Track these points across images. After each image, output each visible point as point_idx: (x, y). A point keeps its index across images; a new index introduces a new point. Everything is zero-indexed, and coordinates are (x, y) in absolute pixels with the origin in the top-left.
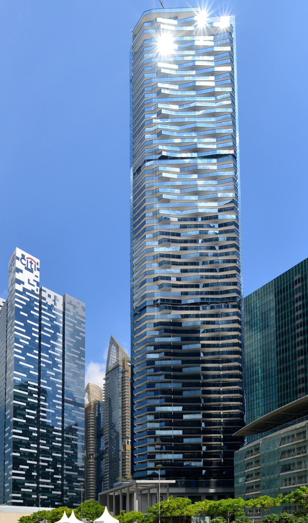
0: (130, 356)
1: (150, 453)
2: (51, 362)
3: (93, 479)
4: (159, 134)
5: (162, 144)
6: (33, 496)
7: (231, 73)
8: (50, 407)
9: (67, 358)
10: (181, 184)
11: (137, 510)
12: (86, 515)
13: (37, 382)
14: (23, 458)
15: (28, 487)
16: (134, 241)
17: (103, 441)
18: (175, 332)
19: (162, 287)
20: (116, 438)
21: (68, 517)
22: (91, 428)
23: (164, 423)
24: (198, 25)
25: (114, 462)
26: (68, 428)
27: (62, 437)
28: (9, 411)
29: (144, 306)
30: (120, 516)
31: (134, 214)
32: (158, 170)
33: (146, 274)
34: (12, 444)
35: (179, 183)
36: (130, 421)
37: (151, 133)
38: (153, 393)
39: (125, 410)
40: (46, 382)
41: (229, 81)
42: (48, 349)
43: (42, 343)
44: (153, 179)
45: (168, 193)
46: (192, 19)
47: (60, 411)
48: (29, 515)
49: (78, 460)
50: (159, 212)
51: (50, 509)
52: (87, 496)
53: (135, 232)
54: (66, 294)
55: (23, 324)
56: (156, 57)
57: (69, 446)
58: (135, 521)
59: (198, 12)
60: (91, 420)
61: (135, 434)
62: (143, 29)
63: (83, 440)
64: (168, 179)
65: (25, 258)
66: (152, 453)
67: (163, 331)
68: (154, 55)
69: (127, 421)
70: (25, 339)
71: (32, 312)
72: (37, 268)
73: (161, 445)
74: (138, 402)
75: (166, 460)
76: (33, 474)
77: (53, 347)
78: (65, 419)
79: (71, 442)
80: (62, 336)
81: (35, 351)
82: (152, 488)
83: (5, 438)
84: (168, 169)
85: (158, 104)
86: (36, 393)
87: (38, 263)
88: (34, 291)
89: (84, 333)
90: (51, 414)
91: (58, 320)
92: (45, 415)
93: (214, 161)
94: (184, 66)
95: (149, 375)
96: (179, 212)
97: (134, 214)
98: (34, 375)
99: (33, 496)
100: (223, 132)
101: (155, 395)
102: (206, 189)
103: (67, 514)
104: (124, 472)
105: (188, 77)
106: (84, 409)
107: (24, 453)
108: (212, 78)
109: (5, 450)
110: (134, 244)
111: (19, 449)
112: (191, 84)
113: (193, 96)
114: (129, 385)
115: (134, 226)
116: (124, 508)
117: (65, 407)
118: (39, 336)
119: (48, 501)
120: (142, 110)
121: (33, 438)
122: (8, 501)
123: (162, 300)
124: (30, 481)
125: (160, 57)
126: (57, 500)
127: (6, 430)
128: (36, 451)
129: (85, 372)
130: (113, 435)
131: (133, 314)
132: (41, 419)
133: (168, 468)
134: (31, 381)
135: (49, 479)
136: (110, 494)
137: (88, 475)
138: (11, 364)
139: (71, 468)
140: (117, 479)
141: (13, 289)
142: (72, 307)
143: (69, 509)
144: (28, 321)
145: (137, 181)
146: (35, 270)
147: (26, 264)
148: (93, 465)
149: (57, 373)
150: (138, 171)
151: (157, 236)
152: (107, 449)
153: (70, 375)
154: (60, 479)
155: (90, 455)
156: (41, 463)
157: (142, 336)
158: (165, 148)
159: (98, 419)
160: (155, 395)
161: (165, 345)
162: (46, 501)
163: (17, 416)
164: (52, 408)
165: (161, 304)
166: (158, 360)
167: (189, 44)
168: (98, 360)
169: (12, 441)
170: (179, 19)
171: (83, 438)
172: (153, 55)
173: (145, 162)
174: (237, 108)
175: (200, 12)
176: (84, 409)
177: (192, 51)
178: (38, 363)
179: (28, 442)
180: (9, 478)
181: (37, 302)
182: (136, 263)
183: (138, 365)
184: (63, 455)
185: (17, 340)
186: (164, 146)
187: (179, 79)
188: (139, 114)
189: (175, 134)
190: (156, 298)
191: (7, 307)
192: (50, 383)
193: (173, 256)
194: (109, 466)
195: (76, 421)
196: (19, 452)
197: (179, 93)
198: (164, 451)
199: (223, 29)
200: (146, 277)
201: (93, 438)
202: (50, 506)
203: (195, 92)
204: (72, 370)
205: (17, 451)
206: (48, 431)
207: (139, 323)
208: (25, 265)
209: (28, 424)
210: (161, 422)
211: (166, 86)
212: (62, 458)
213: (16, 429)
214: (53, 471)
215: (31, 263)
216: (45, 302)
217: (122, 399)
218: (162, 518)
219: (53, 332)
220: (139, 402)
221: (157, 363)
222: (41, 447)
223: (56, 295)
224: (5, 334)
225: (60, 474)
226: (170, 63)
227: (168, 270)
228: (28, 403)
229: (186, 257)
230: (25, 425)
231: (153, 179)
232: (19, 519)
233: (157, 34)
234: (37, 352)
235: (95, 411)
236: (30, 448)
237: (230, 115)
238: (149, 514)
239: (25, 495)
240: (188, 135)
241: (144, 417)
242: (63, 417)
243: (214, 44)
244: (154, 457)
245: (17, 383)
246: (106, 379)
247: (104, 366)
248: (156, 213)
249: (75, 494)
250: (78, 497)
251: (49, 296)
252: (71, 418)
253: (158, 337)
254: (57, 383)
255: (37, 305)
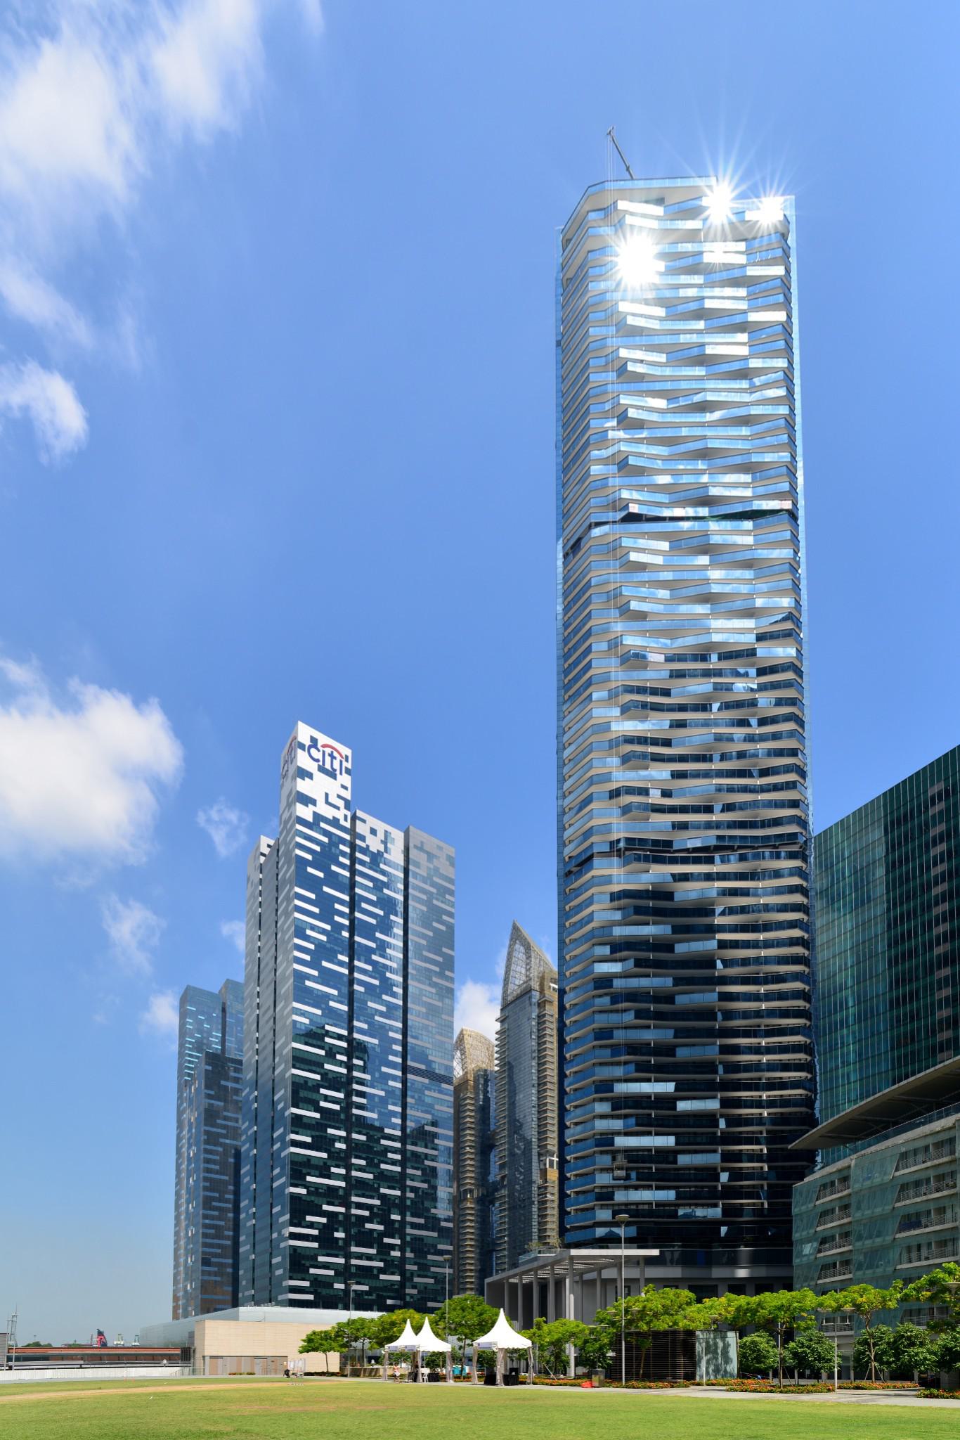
0: (556, 969)
1: (602, 1187)
2: (376, 982)
3: (471, 1246)
4: (623, 465)
5: (630, 487)
6: (337, 1286)
7: (786, 326)
8: (376, 1084)
9: (414, 972)
10: (671, 579)
11: (572, 1318)
12: (455, 1329)
13: (346, 1026)
14: (313, 1198)
15: (326, 1266)
16: (565, 707)
17: (495, 1160)
18: (659, 913)
19: (630, 811)
20: (523, 1153)
21: (416, 1334)
22: (468, 1132)
23: (632, 1121)
24: (711, 217)
25: (520, 1207)
26: (415, 1132)
27: (402, 1151)
28: (282, 1092)
29: (589, 854)
30: (534, 1330)
31: (565, 645)
32: (621, 546)
33: (592, 781)
34: (288, 1168)
35: (667, 576)
36: (555, 1115)
37: (605, 461)
38: (608, 1051)
39: (545, 1091)
40: (365, 1026)
41: (782, 344)
42: (371, 951)
43: (357, 939)
44: (608, 566)
45: (643, 599)
46: (697, 202)
47: (399, 1093)
48: (328, 1328)
49: (439, 1205)
50: (622, 641)
51: (374, 1315)
52: (457, 1285)
53: (566, 687)
54: (411, 827)
55: (313, 896)
56: (615, 291)
57: (419, 1173)
58: (567, 1342)
59: (710, 187)
60: (468, 1113)
61: (567, 1144)
62: (586, 225)
63: (449, 1158)
64: (642, 567)
65: (319, 746)
66: (607, 1187)
67: (632, 910)
68: (611, 285)
69: (549, 1114)
70: (318, 930)
71: (334, 868)
72: (346, 768)
73: (627, 1169)
74: (576, 1072)
75: (637, 1204)
76: (337, 1235)
77: (382, 947)
78: (409, 1111)
79: (423, 1162)
80: (401, 921)
81: (341, 957)
82: (606, 1266)
83: (272, 1154)
84: (642, 543)
85: (621, 396)
86: (343, 1051)
87: (347, 757)
88: (338, 820)
89: (451, 915)
90: (376, 1099)
91: (392, 885)
92: (363, 1101)
93: (748, 525)
94: (678, 309)
95: (601, 1012)
96: (668, 642)
97: (565, 646)
98: (339, 1012)
99: (337, 1286)
100: (766, 460)
101: (613, 1056)
102: (727, 589)
103: (413, 1327)
104: (542, 1230)
105: (688, 336)
106: (451, 1088)
107: (317, 1189)
108: (743, 337)
109: (272, 1180)
110: (566, 713)
111: (305, 1178)
112: (695, 352)
113: (700, 378)
114: (555, 1033)
115: (566, 672)
116: (543, 1313)
117: (409, 1084)
118: (350, 923)
119: (370, 1297)
120: (584, 424)
121: (337, 1153)
122: (280, 1298)
123: (628, 840)
124: (329, 1251)
125: (625, 291)
126: (392, 1294)
127: (275, 1135)
128: (343, 1184)
129: (455, 1004)
130: (519, 1148)
131: (562, 873)
132: (355, 1111)
133: (642, 1222)
134: (331, 1025)
135: (372, 1247)
136: (511, 1280)
137: (461, 1237)
138: (287, 986)
139: (422, 1221)
140: (526, 1246)
141: (290, 817)
142: (426, 856)
143: (417, 1316)
144: (326, 889)
145: (572, 572)
146: (341, 773)
147: (321, 759)
148: (472, 1215)
149: (390, 1007)
150: (574, 548)
151: (617, 696)
152: (503, 1178)
153: (419, 1011)
154: (397, 1248)
155: (465, 1191)
156: (354, 1211)
157: (583, 923)
158: (636, 495)
159: (484, 1110)
160: (613, 1056)
161: (635, 943)
162: (366, 1297)
163: (301, 1105)
164: (379, 1085)
165: (626, 849)
166: (621, 977)
167: (690, 261)
168: (483, 978)
169: (288, 1161)
170: (666, 203)
171: (449, 1154)
172: (610, 284)
173: (590, 527)
174: (798, 404)
175: (715, 188)
176: (451, 1088)
177: (696, 276)
178: (347, 984)
179: (325, 1163)
180: (282, 1245)
181: (344, 845)
182: (571, 757)
183: (575, 988)
184: (405, 1192)
185: (300, 932)
186: (634, 492)
187: (668, 340)
188: (577, 419)
189: (657, 464)
190: (615, 837)
191: (278, 855)
192: (375, 1030)
193: (655, 742)
194: (509, 1218)
195: (433, 1115)
196: (305, 1187)
197: (668, 372)
198: (634, 1182)
199: (768, 225)
200: (593, 789)
201: (472, 1153)
202: (375, 1307)
203: (704, 368)
204: (424, 999)
205: (299, 1182)
206: (369, 1137)
207: (578, 892)
208: (317, 761)
209: (326, 1122)
210: (626, 1116)
211: (639, 355)
212: (403, 1198)
213: (297, 1133)
214: (381, 1228)
215: (333, 757)
216: (363, 845)
217: (538, 1064)
218: (628, 1335)
219: (381, 913)
220: (576, 1072)
221: (617, 983)
222: (354, 1173)
223: (390, 829)
224: (273, 917)
225: (397, 1236)
226: (647, 302)
227: (643, 773)
228: (325, 1075)
229: (683, 744)
230: (317, 1123)
231: (608, 566)
232: (304, 1338)
233: (618, 237)
234: (346, 959)
235: (477, 1094)
236: (329, 1176)
237: (782, 422)
238: (599, 1327)
239: (317, 1282)
240: (689, 467)
241: (588, 1107)
242: (404, 1106)
243: (748, 260)
244: (610, 1196)
245: (301, 1029)
246: (502, 1021)
247: (498, 991)
248: (615, 644)
249: (432, 1281)
250: (439, 1287)
251: (373, 832)
252: (424, 1109)
253: (619, 924)
254: (392, 1028)
255: (346, 853)
